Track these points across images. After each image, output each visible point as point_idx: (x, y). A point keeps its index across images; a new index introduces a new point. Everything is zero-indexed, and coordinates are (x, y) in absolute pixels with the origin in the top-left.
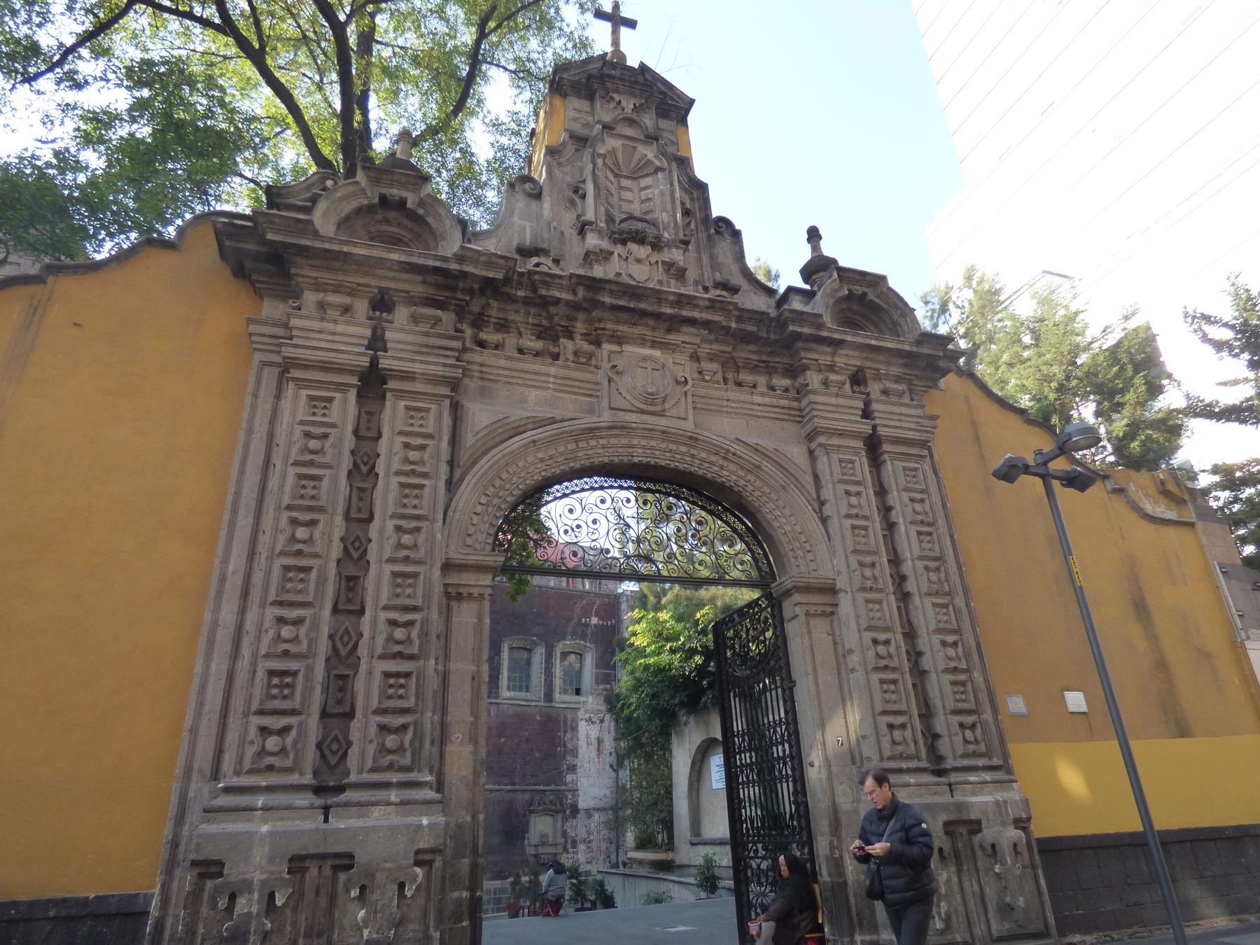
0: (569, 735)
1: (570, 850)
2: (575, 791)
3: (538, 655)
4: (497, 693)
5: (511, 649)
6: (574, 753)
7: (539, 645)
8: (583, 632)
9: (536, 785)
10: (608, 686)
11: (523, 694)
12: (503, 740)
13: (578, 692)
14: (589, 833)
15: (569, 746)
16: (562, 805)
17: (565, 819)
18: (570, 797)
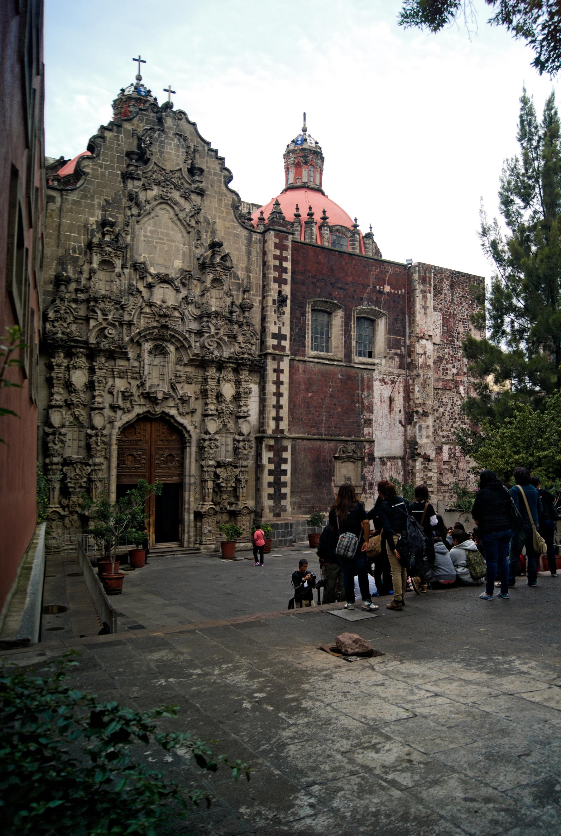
0: (365, 393)
1: (368, 491)
4: (304, 351)
6: (370, 410)
7: (340, 308)
10: (399, 351)
12: (310, 395)
13: (370, 355)
15: (366, 403)
16: (362, 454)
17: (364, 465)
18: (367, 446)
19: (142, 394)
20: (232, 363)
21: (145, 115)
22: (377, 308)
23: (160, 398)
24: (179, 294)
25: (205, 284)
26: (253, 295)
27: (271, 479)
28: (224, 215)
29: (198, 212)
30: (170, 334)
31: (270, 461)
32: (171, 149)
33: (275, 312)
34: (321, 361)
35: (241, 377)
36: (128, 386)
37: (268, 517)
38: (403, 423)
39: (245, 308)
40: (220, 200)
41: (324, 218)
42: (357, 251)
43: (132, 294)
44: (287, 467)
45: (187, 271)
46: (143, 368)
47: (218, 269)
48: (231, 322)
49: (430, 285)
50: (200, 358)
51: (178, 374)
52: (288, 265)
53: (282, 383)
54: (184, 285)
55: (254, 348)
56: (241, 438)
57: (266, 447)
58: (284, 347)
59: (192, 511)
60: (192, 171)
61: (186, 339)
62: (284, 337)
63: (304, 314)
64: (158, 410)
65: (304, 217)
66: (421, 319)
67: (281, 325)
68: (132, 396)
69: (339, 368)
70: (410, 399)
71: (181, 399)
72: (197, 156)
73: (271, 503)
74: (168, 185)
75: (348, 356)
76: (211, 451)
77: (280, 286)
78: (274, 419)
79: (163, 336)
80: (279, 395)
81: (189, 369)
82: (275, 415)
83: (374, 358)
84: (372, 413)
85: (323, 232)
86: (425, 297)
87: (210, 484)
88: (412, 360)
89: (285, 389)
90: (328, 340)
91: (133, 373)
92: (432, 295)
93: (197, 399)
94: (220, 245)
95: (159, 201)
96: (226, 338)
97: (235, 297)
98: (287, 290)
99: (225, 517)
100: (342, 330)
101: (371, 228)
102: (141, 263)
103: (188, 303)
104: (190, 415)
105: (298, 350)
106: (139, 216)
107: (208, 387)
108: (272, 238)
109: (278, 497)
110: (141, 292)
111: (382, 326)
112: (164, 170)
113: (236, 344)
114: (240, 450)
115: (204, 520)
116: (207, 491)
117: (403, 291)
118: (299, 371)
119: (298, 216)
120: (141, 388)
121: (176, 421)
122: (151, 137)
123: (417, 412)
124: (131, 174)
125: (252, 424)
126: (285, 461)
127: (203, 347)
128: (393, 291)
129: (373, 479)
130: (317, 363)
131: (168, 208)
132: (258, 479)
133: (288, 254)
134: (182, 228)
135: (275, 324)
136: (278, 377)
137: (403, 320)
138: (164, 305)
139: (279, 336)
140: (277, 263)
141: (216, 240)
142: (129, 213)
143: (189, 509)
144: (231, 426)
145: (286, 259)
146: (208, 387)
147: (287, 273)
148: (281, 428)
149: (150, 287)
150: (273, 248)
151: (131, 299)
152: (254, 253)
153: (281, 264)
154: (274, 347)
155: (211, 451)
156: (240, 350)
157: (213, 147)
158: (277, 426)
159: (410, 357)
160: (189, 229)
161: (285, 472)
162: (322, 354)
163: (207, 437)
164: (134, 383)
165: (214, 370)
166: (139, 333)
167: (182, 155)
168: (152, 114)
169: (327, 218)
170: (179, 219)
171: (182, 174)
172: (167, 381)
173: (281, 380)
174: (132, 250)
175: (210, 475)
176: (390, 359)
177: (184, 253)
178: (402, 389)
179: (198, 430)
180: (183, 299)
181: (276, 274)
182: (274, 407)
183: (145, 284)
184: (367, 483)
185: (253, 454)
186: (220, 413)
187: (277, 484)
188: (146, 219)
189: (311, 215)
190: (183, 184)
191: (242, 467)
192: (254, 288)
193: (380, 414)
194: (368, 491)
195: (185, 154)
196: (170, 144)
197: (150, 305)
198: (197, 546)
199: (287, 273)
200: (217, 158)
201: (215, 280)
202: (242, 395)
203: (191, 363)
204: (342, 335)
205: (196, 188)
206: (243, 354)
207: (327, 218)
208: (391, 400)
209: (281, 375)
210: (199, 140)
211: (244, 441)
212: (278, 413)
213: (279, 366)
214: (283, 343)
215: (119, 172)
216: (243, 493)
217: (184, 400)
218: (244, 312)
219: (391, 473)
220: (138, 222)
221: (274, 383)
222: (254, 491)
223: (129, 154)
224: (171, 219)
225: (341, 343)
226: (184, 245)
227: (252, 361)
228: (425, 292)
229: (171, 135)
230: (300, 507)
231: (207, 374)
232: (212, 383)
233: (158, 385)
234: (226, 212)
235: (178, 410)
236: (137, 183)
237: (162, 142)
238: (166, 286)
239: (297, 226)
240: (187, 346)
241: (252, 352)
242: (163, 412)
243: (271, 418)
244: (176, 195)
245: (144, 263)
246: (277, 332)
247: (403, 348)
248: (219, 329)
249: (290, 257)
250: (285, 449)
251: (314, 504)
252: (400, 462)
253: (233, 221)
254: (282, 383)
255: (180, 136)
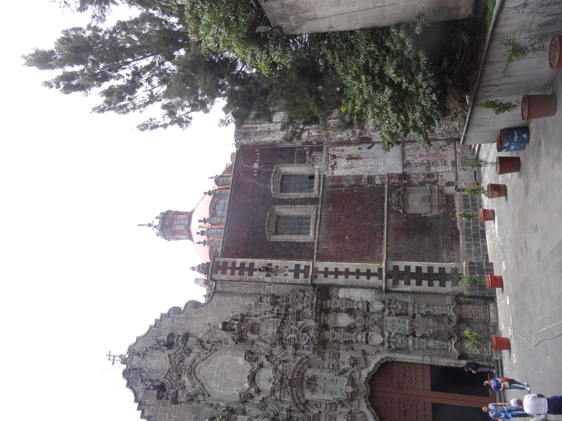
0: (344, 183)
1: (435, 178)
2: (390, 176)
3: (281, 210)
5: (276, 233)
7: (273, 210)
8: (264, 175)
9: (383, 209)
10: (307, 152)
11: (312, 221)
12: (347, 237)
13: (312, 177)
14: (422, 164)
15: (353, 182)
17: (410, 184)
18: (393, 181)
19: (349, 403)
20: (320, 316)
21: (132, 380)
22: (272, 175)
23: (352, 390)
24: (264, 363)
25: (255, 339)
26: (264, 291)
27: (425, 283)
28: (203, 315)
29: (200, 341)
30: (297, 375)
31: (408, 283)
32: (154, 362)
33: (277, 275)
34: (317, 227)
35: (332, 308)
36: (342, 415)
37: (463, 287)
38: (371, 145)
39: (275, 299)
40: (192, 319)
41: (205, 221)
42: (229, 191)
43: (266, 405)
44: (413, 265)
45: (245, 356)
46: (326, 400)
47: (243, 327)
48: (286, 315)
49: (250, 128)
50: (317, 347)
51: (331, 367)
52: (239, 261)
53: (336, 269)
54: (257, 359)
55: (307, 294)
56: (387, 311)
57: (395, 287)
58: (305, 266)
59: (457, 362)
60: (170, 345)
61: (300, 362)
62: (297, 266)
63: (278, 243)
64: (364, 389)
65: (204, 238)
66: (279, 135)
67: (287, 269)
68: (350, 412)
69: (324, 209)
70: (349, 140)
71: (353, 365)
72: (159, 338)
73: (449, 284)
74: (180, 368)
75: (313, 201)
76: (400, 341)
77: (255, 270)
78: (368, 278)
79: (299, 381)
80: (347, 273)
81: (327, 355)
82: (366, 277)
83: (314, 174)
84: (362, 176)
85: (215, 223)
86: (260, 133)
87: (431, 344)
88: (314, 141)
89: (343, 266)
90: (299, 218)
91: (331, 410)
92: (259, 126)
93: (353, 349)
94: (225, 324)
95: (193, 376)
96: (300, 323)
97: (266, 310)
98: (259, 263)
99: (463, 326)
100: (291, 208)
101: (211, 178)
102: (241, 397)
103: (272, 355)
104: (367, 356)
105: (309, 249)
106: (204, 395)
107: (342, 341)
108: (219, 276)
109: (442, 277)
110: (263, 398)
111: (288, 169)
112: (169, 370)
113: (305, 310)
114: (398, 312)
115: (466, 353)
116: (438, 347)
117: (257, 150)
118: (326, 249)
119: (204, 243)
120: (344, 403)
121: (373, 370)
122: (146, 380)
123: (360, 134)
124: (173, 399)
125: (374, 295)
126: (408, 268)
127: (307, 344)
128: (258, 160)
129: (423, 174)
130: (319, 232)
131: (198, 367)
132: (425, 293)
133: (230, 260)
134: (213, 356)
135: (286, 275)
136: (331, 273)
137: (282, 149)
138: (273, 381)
139: (297, 271)
140: (237, 272)
141: (220, 326)
142: (202, 402)
143: (455, 364)
144: (376, 317)
145: (234, 263)
146: (342, 341)
147: (244, 263)
148: (377, 272)
149: (258, 391)
150: (226, 276)
151: (271, 407)
152: (232, 289)
153: (238, 268)
154: (306, 276)
155: (400, 341)
156: (309, 307)
157: (153, 323)
158: (375, 274)
159: (312, 142)
160: (214, 350)
161: (418, 269)
162: (312, 226)
163: (387, 345)
164: (340, 409)
165: (327, 333)
166: (297, 405)
167: (158, 353)
168: (131, 375)
169: (204, 218)
170: (206, 358)
171: (173, 354)
172: (337, 378)
173: (334, 270)
174: (231, 403)
175: (422, 343)
176: (314, 161)
177: (232, 355)
178: (340, 148)
179: (381, 349)
180: (268, 360)
181: (246, 273)
182: (358, 278)
183: (256, 395)
184: (428, 180)
185: (401, 296)
186: (365, 329)
187: (430, 277)
188: (207, 388)
189: (202, 233)
190: (180, 354)
191: (414, 310)
192: (258, 289)
193: (363, 168)
194: (435, 178)
195: (158, 351)
196: (150, 363)
197: (273, 392)
198: (493, 360)
199: (244, 263)
200: (161, 320)
201: (253, 331)
202: (348, 307)
203: (321, 355)
204: (295, 208)
205: (182, 343)
206: (312, 304)
207: (204, 218)
208: (350, 158)
209: (330, 270)
210: (148, 335)
211: (389, 308)
212: (363, 274)
213: (321, 272)
214: (302, 268)
215: (174, 406)
216: (439, 310)
217: (354, 362)
218: (278, 302)
219: (417, 155)
220: (209, 396)
221: (336, 277)
222: (437, 296)
223: (159, 397)
224: (206, 365)
225: (302, 208)
226: (226, 354)
227: (317, 300)
228: (256, 133)
229: (144, 362)
230: (452, 249)
231: (330, 340)
232: (338, 336)
233: (341, 389)
234: (201, 314)
235: (363, 368)
236: (180, 394)
237: (149, 371)
238: (257, 376)
239: (213, 244)
240: (307, 360)
241: (310, 296)
242: (365, 383)
243: (368, 280)
244: (188, 360)
245: (240, 395)
246: (293, 273)
247: (305, 149)
248: (292, 330)
249: (232, 260)
250: (396, 268)
251: (448, 235)
252: (407, 147)
253: (207, 307)
254: (336, 269)
255: (144, 354)
